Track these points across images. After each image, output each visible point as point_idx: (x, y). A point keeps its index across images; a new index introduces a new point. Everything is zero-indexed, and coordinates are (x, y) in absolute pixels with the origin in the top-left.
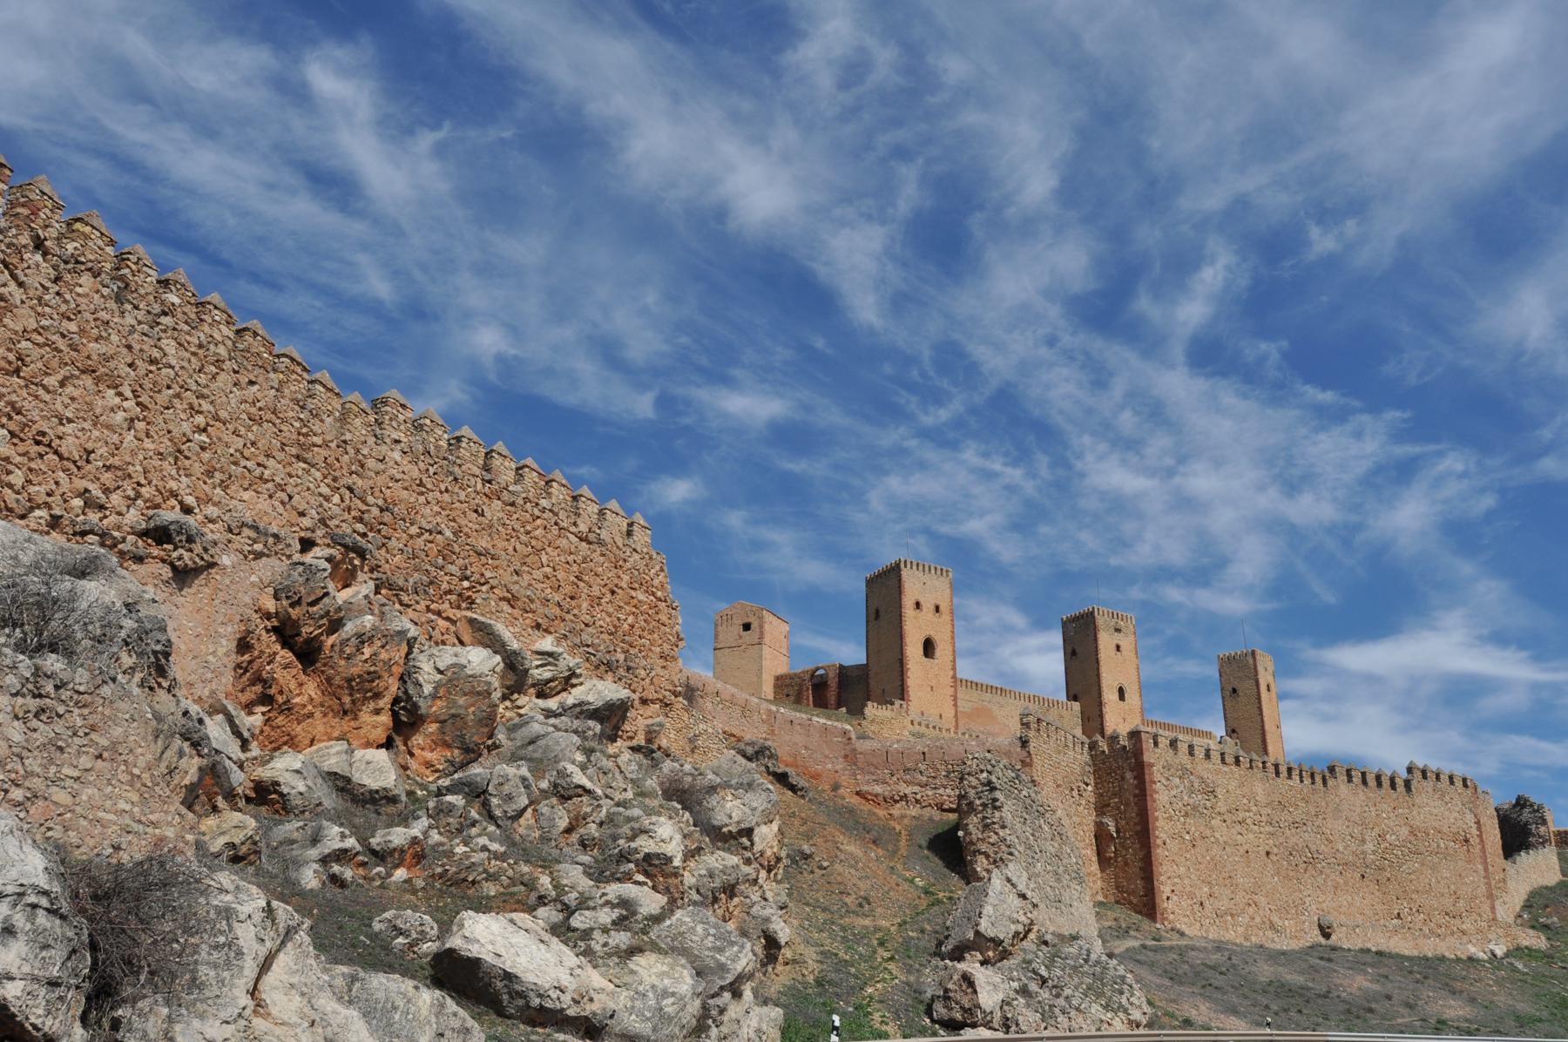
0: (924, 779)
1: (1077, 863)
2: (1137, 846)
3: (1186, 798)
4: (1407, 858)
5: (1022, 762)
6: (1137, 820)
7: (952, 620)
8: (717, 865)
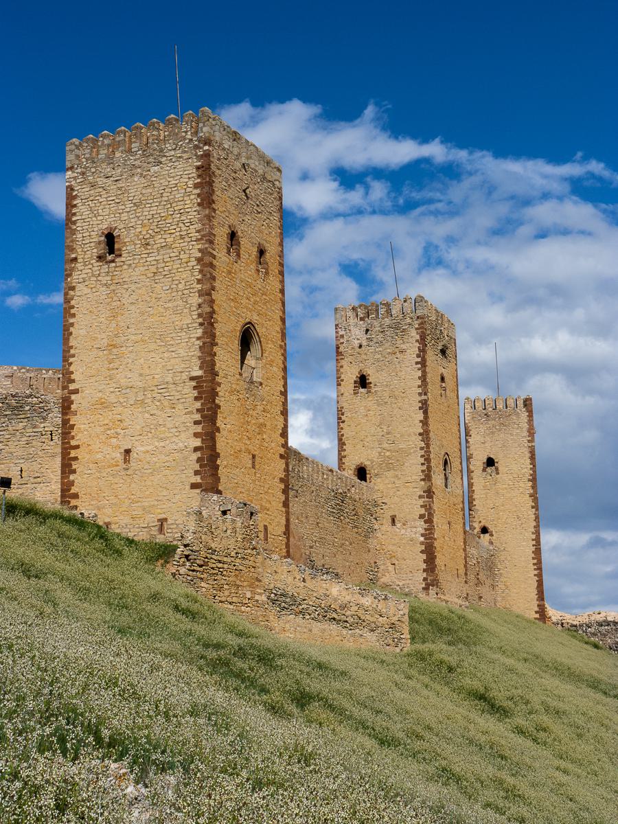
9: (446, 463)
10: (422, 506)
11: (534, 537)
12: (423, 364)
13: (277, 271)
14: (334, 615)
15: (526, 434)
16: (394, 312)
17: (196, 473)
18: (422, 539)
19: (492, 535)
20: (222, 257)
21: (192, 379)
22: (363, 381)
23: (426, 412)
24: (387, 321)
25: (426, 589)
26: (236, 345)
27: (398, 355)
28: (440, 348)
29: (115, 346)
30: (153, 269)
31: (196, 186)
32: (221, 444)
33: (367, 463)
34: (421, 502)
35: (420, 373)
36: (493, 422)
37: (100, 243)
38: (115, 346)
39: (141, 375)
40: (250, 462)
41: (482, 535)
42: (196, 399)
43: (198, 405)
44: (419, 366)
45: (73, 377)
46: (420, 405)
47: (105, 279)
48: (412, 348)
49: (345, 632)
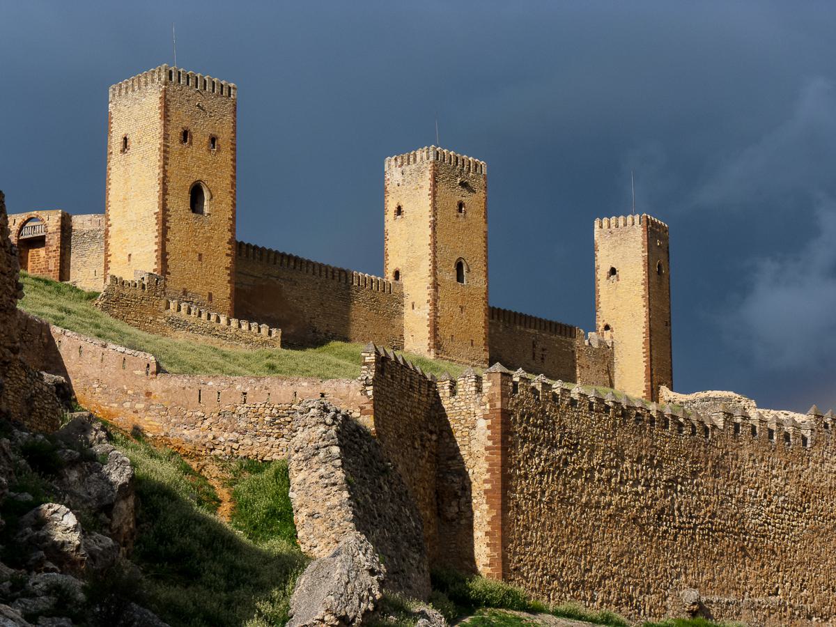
0: (243, 424)
1: (416, 527)
2: (486, 507)
3: (545, 451)
4: (794, 523)
5: (362, 408)
6: (487, 476)
7: (234, 160)
8: (97, 547)
9: (459, 266)
10: (429, 294)
11: (644, 330)
12: (434, 195)
13: (229, 149)
14: (217, 333)
15: (641, 246)
16: (417, 159)
17: (156, 263)
18: (428, 317)
19: (612, 331)
20: (175, 145)
21: (155, 214)
22: (399, 211)
23: (434, 229)
24: (413, 166)
25: (429, 351)
26: (187, 196)
27: (419, 190)
28: (458, 182)
29: (126, 199)
30: (141, 155)
31: (159, 108)
32: (169, 247)
33: (400, 267)
34: (428, 291)
35: (430, 202)
36: (616, 238)
37: (121, 143)
38: (126, 199)
39: (136, 214)
40: (197, 258)
41: (605, 332)
42: (156, 224)
43: (157, 227)
44: (430, 197)
45: (109, 217)
46: (430, 224)
47: (123, 163)
48: (427, 182)
49: (224, 342)
